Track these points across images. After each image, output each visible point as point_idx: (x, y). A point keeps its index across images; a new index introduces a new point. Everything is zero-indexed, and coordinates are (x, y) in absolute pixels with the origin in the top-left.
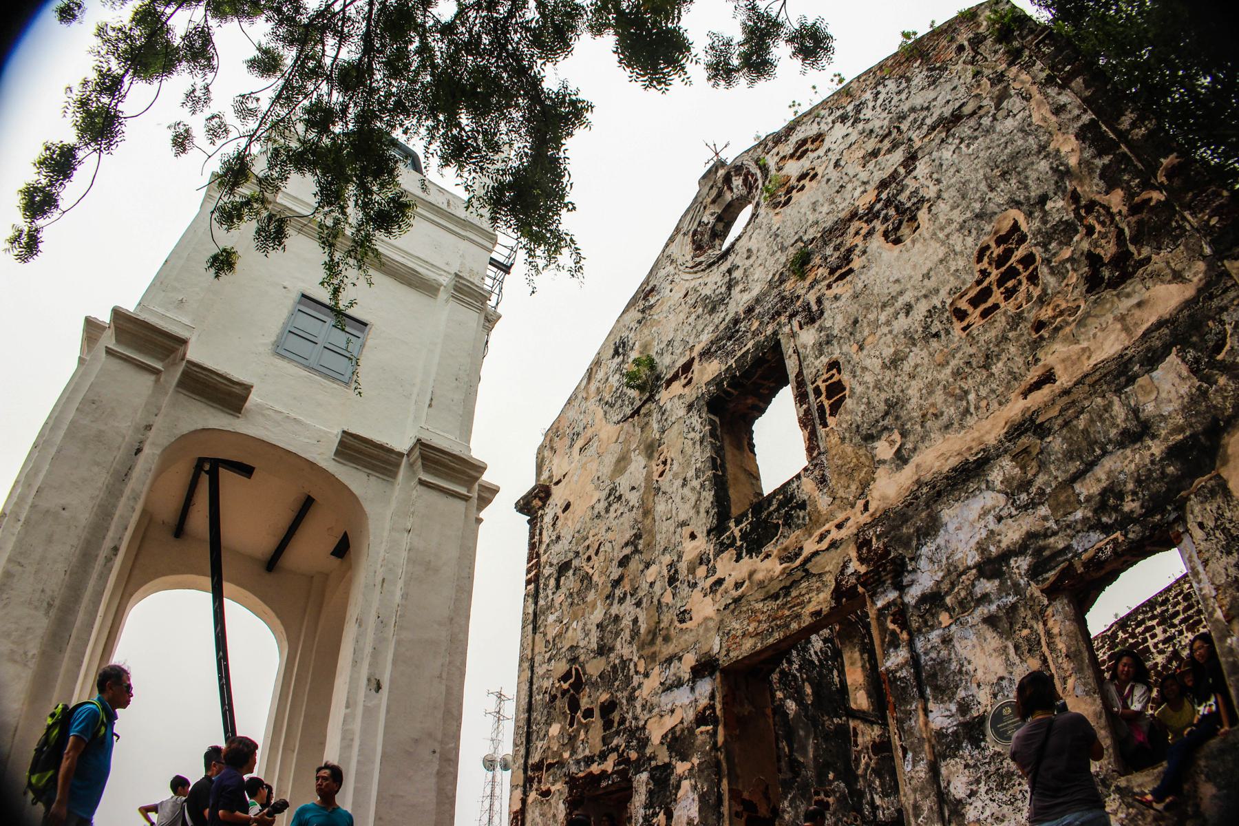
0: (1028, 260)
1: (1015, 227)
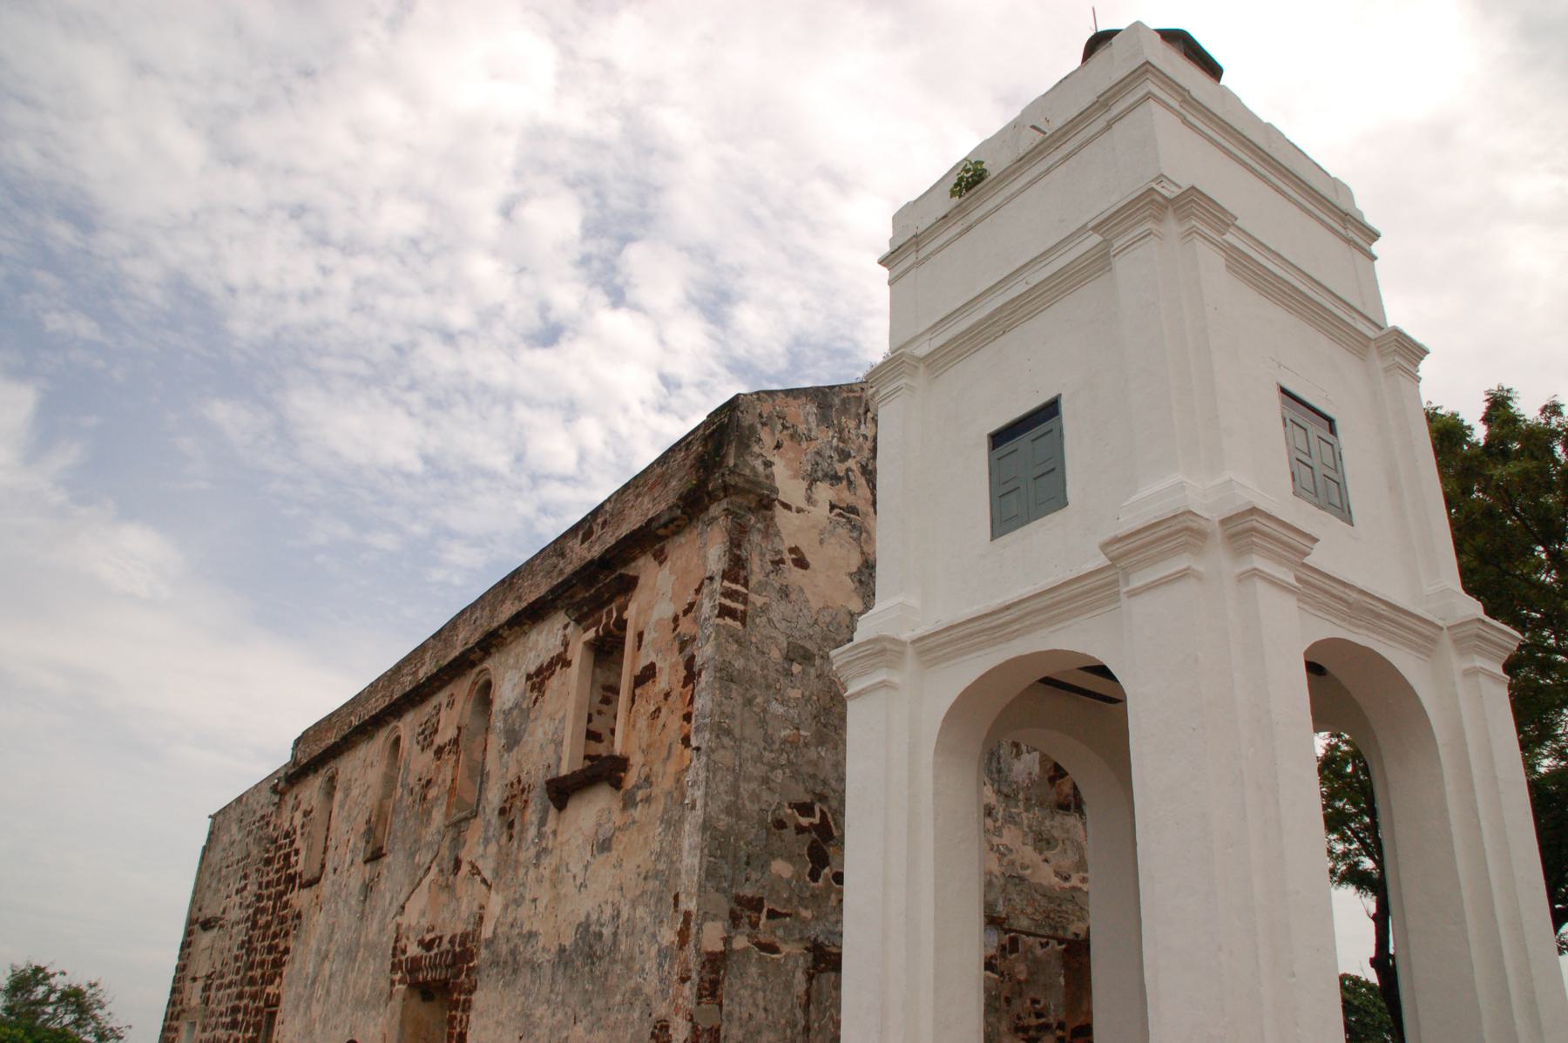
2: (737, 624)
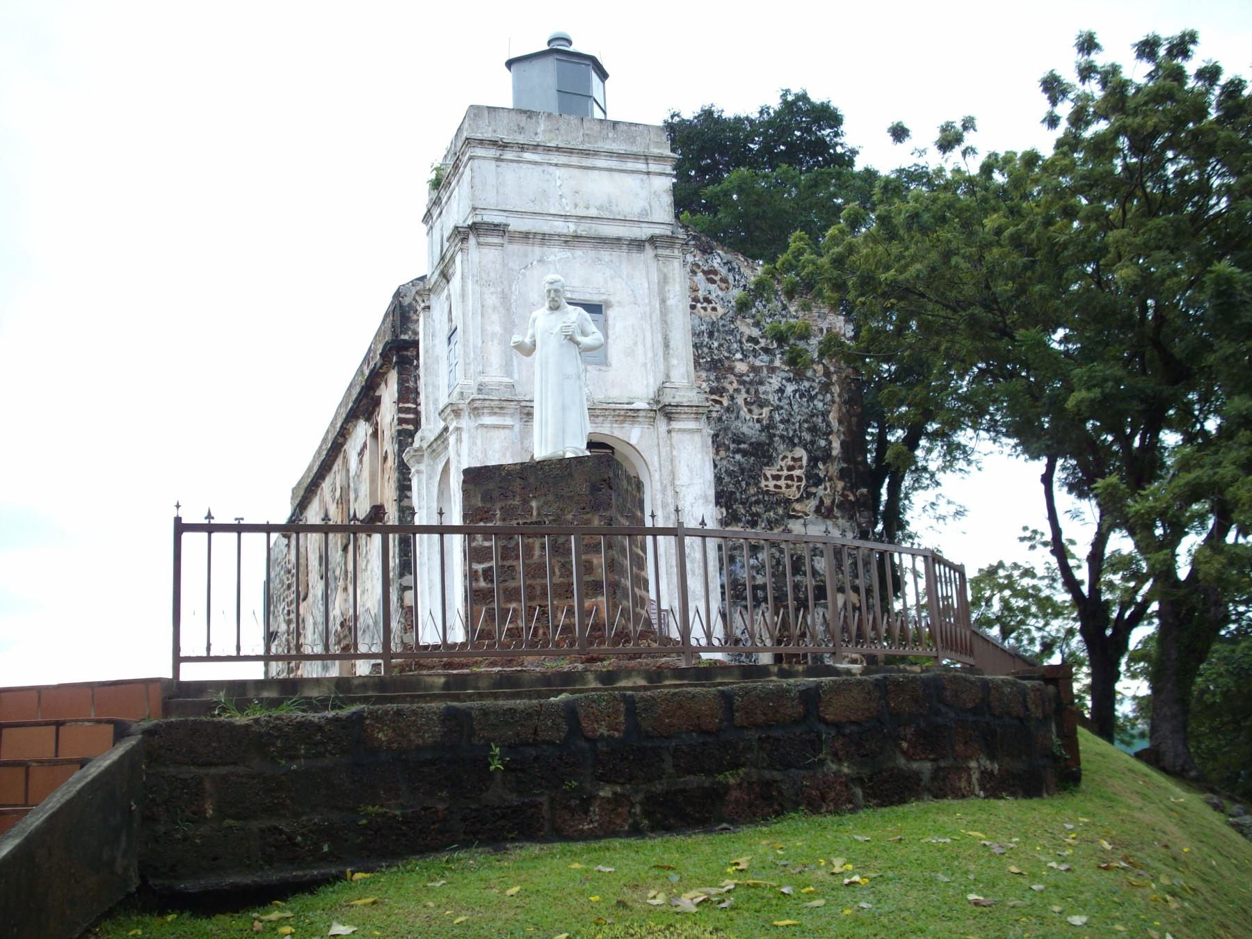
0: (800, 479)
1: (800, 459)
2: (411, 427)
